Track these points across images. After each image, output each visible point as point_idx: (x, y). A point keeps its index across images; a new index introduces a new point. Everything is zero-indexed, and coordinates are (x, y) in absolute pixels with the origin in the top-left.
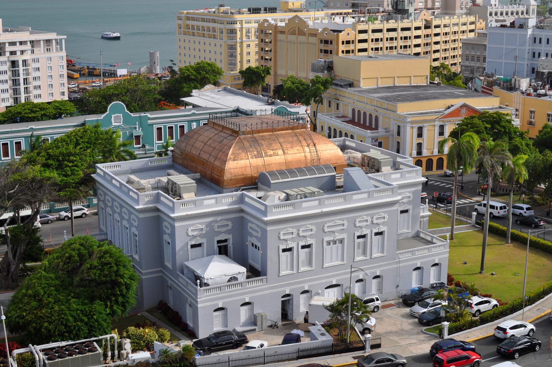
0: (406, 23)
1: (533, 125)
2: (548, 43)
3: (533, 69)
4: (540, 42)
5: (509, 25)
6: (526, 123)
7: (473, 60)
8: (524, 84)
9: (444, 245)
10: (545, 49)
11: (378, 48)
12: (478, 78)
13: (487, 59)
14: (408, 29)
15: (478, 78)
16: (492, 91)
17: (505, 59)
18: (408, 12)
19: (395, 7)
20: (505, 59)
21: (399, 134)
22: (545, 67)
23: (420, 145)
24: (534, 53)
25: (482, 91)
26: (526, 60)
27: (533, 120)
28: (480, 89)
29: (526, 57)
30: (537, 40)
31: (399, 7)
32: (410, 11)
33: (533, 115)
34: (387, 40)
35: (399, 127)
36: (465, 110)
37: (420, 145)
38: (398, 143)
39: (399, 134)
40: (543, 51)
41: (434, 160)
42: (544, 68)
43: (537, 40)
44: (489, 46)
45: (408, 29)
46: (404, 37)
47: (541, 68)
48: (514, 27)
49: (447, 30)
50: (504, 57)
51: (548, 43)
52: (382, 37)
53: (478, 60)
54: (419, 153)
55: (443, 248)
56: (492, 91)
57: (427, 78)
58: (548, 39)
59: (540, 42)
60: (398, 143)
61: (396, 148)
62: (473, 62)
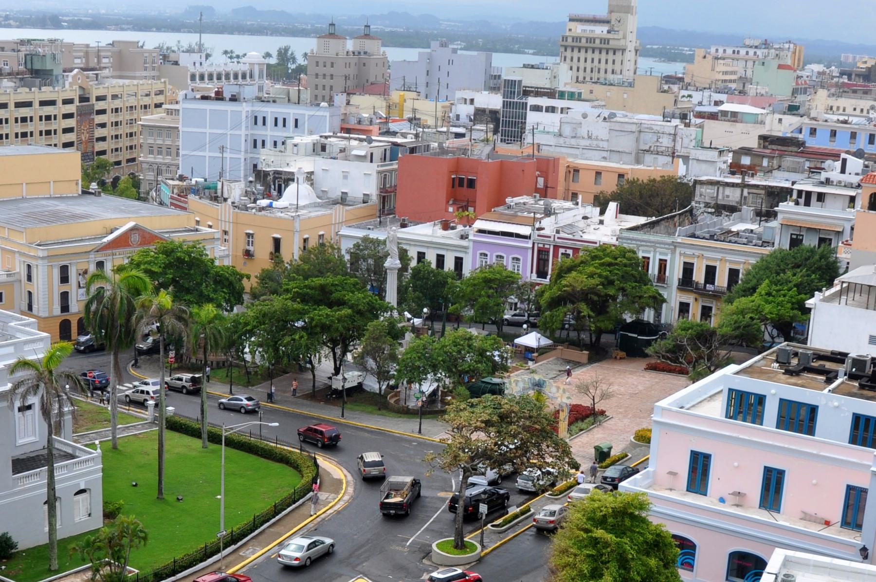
0: (47, 93)
1: (252, 256)
2: (296, 126)
3: (255, 166)
4: (264, 124)
5: (213, 95)
6: (240, 253)
7: (160, 153)
8: (235, 191)
9: (93, 459)
10: (272, 133)
11: (50, 131)
12: (165, 184)
13: (180, 151)
14: (52, 103)
15: (165, 184)
16: (186, 203)
17: (210, 151)
18: (52, 75)
19: (29, 66)
20: (210, 151)
21: (29, 278)
22: (270, 163)
23: (65, 296)
24: (255, 141)
25: (172, 204)
26: (243, 153)
27: (251, 248)
28: (167, 201)
29: (243, 149)
30: (260, 121)
31: (37, 66)
32: (55, 73)
33: (251, 240)
34: (41, 119)
35: (29, 266)
36: (137, 235)
37: (65, 296)
38: (30, 293)
39: (29, 278)
40: (269, 138)
41: (72, 322)
42: (268, 165)
43: (260, 121)
44: (185, 129)
45: (52, 103)
46: (46, 116)
47: (264, 165)
48: (222, 99)
49: (117, 103)
50: (207, 146)
51: (296, 126)
52: (7, 116)
53: (169, 154)
54: (65, 308)
55: (91, 464)
56: (186, 203)
57: (77, 184)
58: (296, 121)
59: (264, 124)
60: (30, 293)
61: (27, 302)
62: (159, 156)
